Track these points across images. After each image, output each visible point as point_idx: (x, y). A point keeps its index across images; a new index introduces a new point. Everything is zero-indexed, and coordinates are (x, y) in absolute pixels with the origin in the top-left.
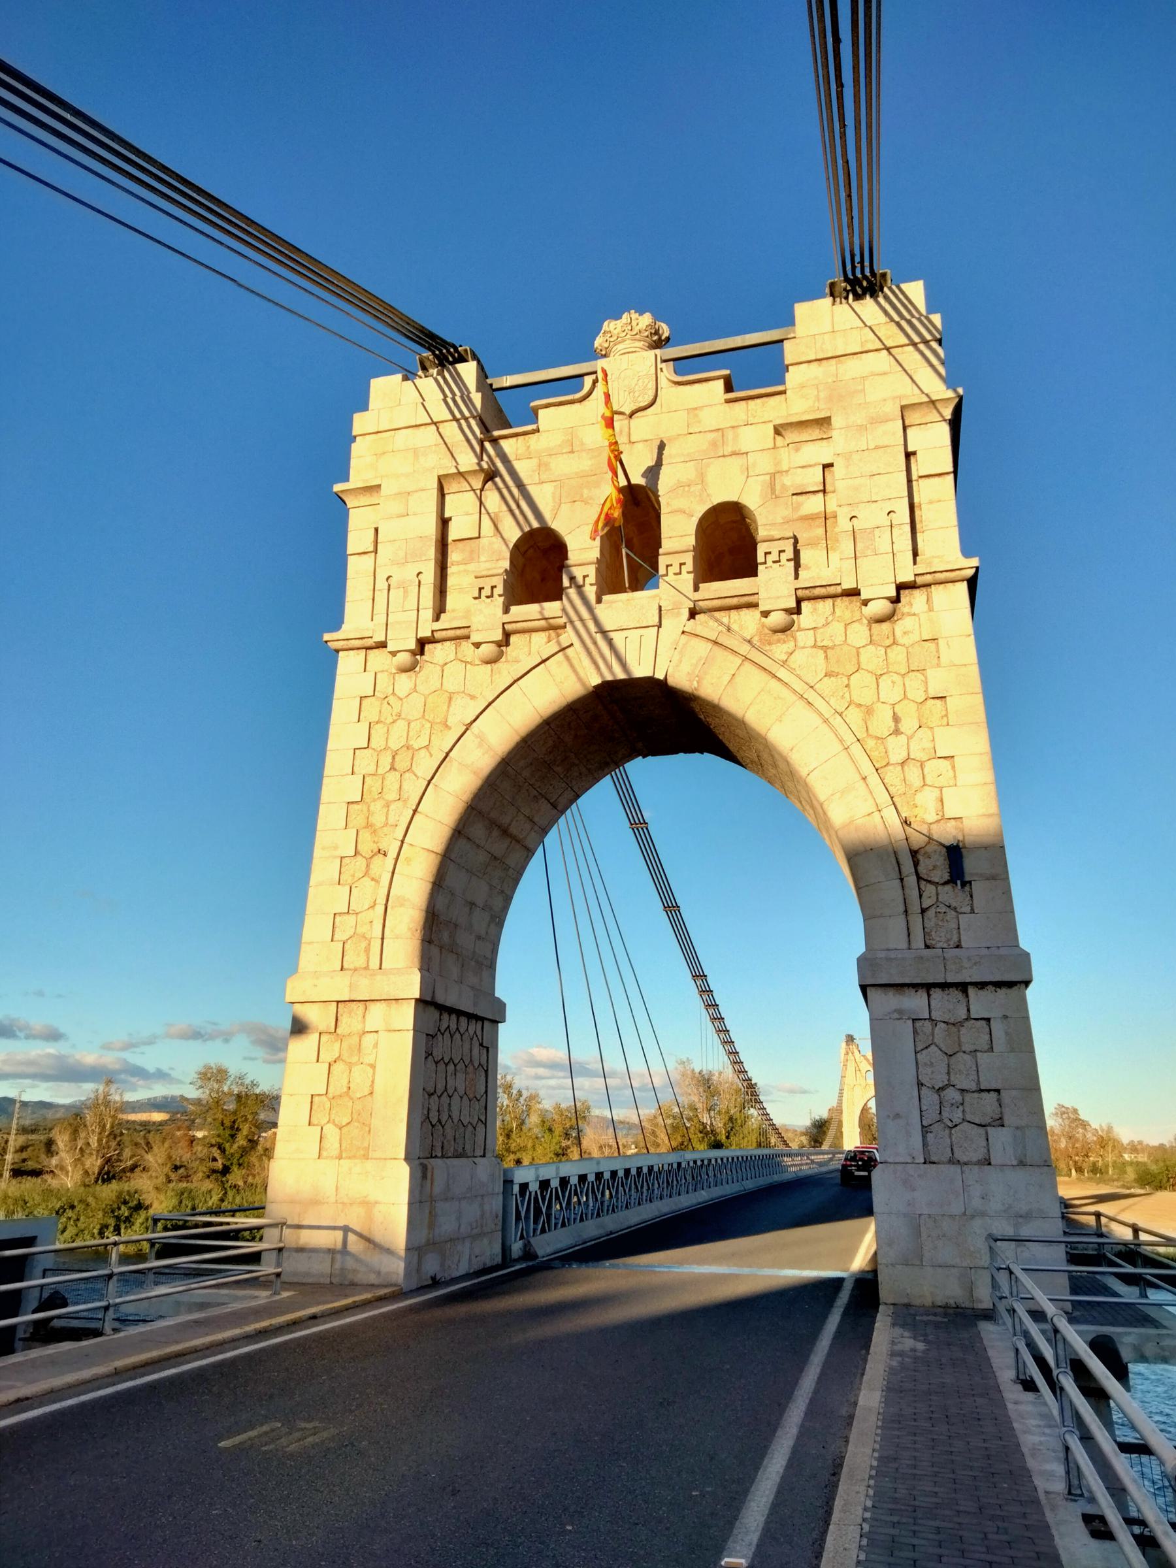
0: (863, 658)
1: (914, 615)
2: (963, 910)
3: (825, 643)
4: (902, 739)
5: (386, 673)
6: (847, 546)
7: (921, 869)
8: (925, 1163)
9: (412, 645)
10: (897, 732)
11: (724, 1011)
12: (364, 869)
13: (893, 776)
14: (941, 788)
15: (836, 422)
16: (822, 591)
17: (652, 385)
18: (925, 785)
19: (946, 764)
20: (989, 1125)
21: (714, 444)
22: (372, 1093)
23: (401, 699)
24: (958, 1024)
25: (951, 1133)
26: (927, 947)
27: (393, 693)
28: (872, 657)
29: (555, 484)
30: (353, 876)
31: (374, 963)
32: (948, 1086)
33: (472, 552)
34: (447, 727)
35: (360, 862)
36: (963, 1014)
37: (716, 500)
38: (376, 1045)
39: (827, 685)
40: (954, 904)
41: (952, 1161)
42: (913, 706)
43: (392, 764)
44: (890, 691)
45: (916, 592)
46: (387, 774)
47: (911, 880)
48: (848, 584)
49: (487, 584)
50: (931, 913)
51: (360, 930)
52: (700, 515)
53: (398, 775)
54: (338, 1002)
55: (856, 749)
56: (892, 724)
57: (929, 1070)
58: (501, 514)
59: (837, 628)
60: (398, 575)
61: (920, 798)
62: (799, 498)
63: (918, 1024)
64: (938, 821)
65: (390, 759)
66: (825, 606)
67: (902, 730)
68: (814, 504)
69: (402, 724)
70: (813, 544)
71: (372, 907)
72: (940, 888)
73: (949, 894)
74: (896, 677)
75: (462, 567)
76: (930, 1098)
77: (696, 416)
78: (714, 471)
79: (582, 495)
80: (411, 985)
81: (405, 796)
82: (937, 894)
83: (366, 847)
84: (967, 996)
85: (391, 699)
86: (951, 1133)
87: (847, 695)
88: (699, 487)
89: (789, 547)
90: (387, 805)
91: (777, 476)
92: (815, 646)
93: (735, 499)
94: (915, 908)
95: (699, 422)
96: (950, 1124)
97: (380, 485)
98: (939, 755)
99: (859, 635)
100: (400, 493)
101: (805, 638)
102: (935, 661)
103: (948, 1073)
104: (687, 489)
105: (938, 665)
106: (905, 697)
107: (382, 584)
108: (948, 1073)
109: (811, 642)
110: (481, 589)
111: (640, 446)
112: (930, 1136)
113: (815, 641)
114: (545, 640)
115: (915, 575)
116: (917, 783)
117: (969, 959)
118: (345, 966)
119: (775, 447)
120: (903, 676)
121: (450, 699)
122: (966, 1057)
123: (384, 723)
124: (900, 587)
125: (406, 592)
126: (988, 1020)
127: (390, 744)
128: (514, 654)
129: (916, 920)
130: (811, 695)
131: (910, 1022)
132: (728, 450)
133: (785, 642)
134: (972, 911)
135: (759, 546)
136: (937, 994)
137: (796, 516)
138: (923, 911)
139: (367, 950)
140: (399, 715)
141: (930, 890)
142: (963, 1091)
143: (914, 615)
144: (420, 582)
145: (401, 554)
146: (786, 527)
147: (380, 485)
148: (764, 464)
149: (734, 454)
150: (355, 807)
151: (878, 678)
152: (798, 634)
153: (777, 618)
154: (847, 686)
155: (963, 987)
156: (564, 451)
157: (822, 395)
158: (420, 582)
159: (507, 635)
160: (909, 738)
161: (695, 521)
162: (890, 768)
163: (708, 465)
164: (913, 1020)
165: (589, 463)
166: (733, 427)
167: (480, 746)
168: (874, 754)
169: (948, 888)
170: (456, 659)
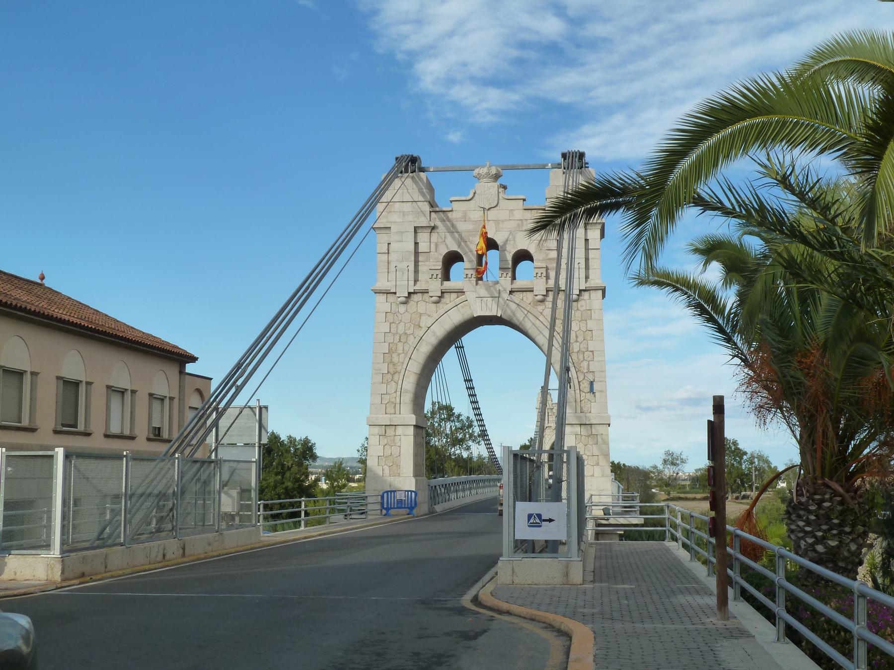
9: (407, 295)
10: (577, 341)
11: (475, 383)
12: (391, 378)
14: (589, 361)
18: (584, 360)
19: (591, 353)
21: (518, 225)
22: (399, 456)
27: (398, 312)
30: (387, 380)
31: (398, 411)
34: (420, 327)
35: (389, 376)
38: (400, 440)
42: (582, 333)
43: (400, 339)
45: (586, 292)
50: (583, 402)
54: (385, 425)
56: (575, 338)
58: (438, 243)
60: (399, 265)
63: (577, 436)
64: (587, 372)
67: (578, 340)
73: (589, 396)
74: (577, 322)
75: (423, 263)
77: (512, 213)
81: (405, 352)
83: (391, 371)
89: (544, 271)
90: (399, 355)
95: (513, 215)
97: (390, 227)
100: (399, 232)
105: (591, 319)
106: (580, 329)
107: (392, 268)
111: (491, 222)
114: (456, 296)
116: (582, 359)
118: (387, 413)
120: (580, 321)
121: (420, 316)
125: (403, 273)
127: (398, 332)
128: (444, 300)
134: (595, 402)
139: (395, 407)
140: (401, 320)
142: (588, 456)
150: (386, 355)
152: (546, 303)
153: (540, 297)
159: (442, 293)
162: (574, 353)
163: (517, 233)
165: (472, 226)
167: (434, 335)
169: (589, 394)
170: (422, 300)
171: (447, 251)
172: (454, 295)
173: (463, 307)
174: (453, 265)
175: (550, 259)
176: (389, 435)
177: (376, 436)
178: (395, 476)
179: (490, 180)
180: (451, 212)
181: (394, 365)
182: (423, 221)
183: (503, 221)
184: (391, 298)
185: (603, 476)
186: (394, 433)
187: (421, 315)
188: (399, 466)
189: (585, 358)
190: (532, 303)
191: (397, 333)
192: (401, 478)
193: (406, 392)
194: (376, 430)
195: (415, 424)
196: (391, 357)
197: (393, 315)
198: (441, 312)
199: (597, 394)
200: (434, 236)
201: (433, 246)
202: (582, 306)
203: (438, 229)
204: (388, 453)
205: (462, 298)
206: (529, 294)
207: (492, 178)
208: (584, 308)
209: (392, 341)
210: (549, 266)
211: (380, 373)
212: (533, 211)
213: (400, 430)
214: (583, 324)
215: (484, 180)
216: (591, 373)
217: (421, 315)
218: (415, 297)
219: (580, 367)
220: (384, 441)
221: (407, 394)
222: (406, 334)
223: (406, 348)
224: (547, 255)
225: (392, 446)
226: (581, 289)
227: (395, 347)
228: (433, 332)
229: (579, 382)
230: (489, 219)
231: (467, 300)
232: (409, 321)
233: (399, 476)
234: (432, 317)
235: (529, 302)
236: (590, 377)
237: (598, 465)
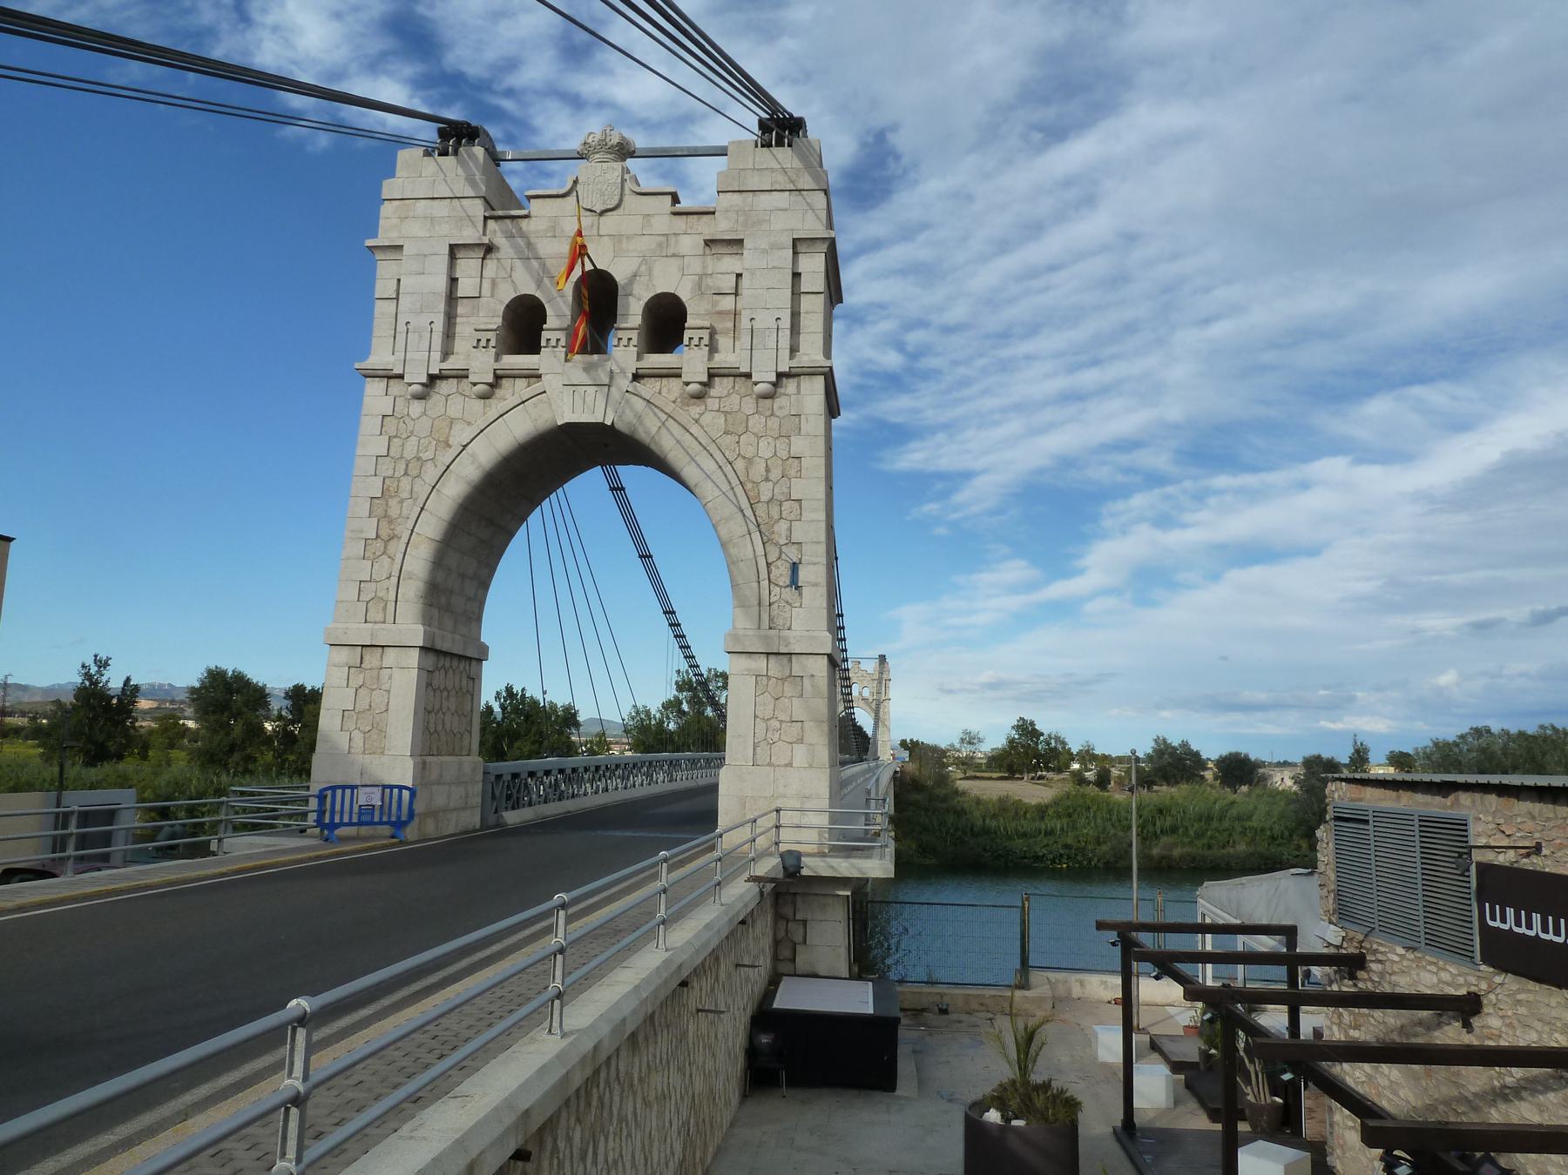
0: (751, 423)
1: (788, 395)
2: (795, 605)
3: (726, 409)
6: (745, 340)
9: (424, 380)
10: (767, 479)
11: (690, 640)
12: (382, 549)
14: (791, 521)
16: (727, 371)
17: (618, 192)
19: (796, 505)
20: (794, 743)
21: (660, 245)
22: (387, 710)
25: (771, 748)
27: (408, 415)
28: (756, 423)
30: (374, 553)
31: (390, 618)
32: (773, 718)
34: (449, 446)
35: (379, 544)
38: (390, 678)
40: (790, 601)
41: (770, 764)
44: (765, 450)
45: (791, 380)
49: (484, 336)
50: (775, 606)
51: (380, 594)
52: (646, 300)
53: (410, 478)
54: (363, 646)
56: (764, 473)
57: (762, 708)
59: (735, 398)
61: (776, 528)
62: (718, 297)
66: (728, 382)
67: (771, 478)
68: (727, 303)
69: (413, 439)
70: (726, 333)
71: (389, 578)
72: (783, 589)
73: (789, 594)
74: (770, 440)
75: (465, 319)
76: (761, 726)
77: (649, 220)
78: (659, 266)
80: (415, 633)
81: (415, 496)
82: (781, 594)
83: (384, 533)
85: (407, 420)
86: (771, 748)
87: (737, 449)
88: (647, 277)
89: (705, 334)
90: (402, 502)
91: (704, 277)
95: (651, 226)
97: (402, 246)
98: (792, 498)
99: (749, 405)
101: (712, 403)
102: (797, 431)
103: (774, 710)
105: (799, 434)
107: (401, 327)
108: (774, 710)
110: (479, 340)
111: (606, 238)
114: (526, 384)
115: (790, 368)
116: (776, 517)
117: (794, 637)
118: (368, 620)
119: (704, 255)
120: (775, 439)
121: (451, 423)
122: (786, 700)
123: (400, 438)
124: (780, 375)
125: (420, 336)
127: (405, 455)
130: (712, 448)
132: (670, 252)
133: (698, 406)
135: (686, 331)
136: (772, 659)
139: (385, 609)
140: (412, 432)
141: (776, 590)
142: (781, 722)
143: (788, 395)
144: (432, 329)
145: (418, 305)
146: (707, 317)
147: (402, 246)
148: (695, 266)
149: (674, 255)
152: (710, 400)
153: (694, 388)
157: (741, 219)
158: (432, 329)
160: (775, 484)
162: (760, 504)
166: (674, 234)
168: (751, 494)
169: (788, 589)
170: (458, 392)
171: (514, 295)
172: (521, 383)
175: (720, 313)
176: (369, 667)
178: (374, 753)
179: (609, 156)
180: (527, 220)
182: (470, 235)
183: (629, 238)
185: (811, 766)
186: (378, 663)
187: (452, 421)
188: (383, 733)
190: (679, 400)
191: (402, 458)
193: (410, 578)
194: (343, 655)
195: (421, 645)
196: (387, 504)
197: (397, 421)
199: (805, 590)
200: (491, 264)
201: (486, 285)
202: (780, 408)
203: (498, 252)
204: (363, 704)
205: (537, 387)
206: (674, 384)
207: (611, 153)
208: (786, 412)
209: (390, 473)
210: (718, 326)
212: (690, 217)
213: (391, 656)
214: (781, 445)
215: (597, 156)
216: (796, 546)
217: (452, 421)
218: (444, 387)
219: (773, 532)
220: (357, 679)
221: (411, 581)
222: (419, 459)
224: (714, 304)
225: (373, 690)
226: (779, 370)
227: (395, 485)
229: (768, 564)
230: (601, 233)
231: (545, 392)
232: (428, 434)
233: (382, 753)
236: (792, 554)
237: (802, 743)
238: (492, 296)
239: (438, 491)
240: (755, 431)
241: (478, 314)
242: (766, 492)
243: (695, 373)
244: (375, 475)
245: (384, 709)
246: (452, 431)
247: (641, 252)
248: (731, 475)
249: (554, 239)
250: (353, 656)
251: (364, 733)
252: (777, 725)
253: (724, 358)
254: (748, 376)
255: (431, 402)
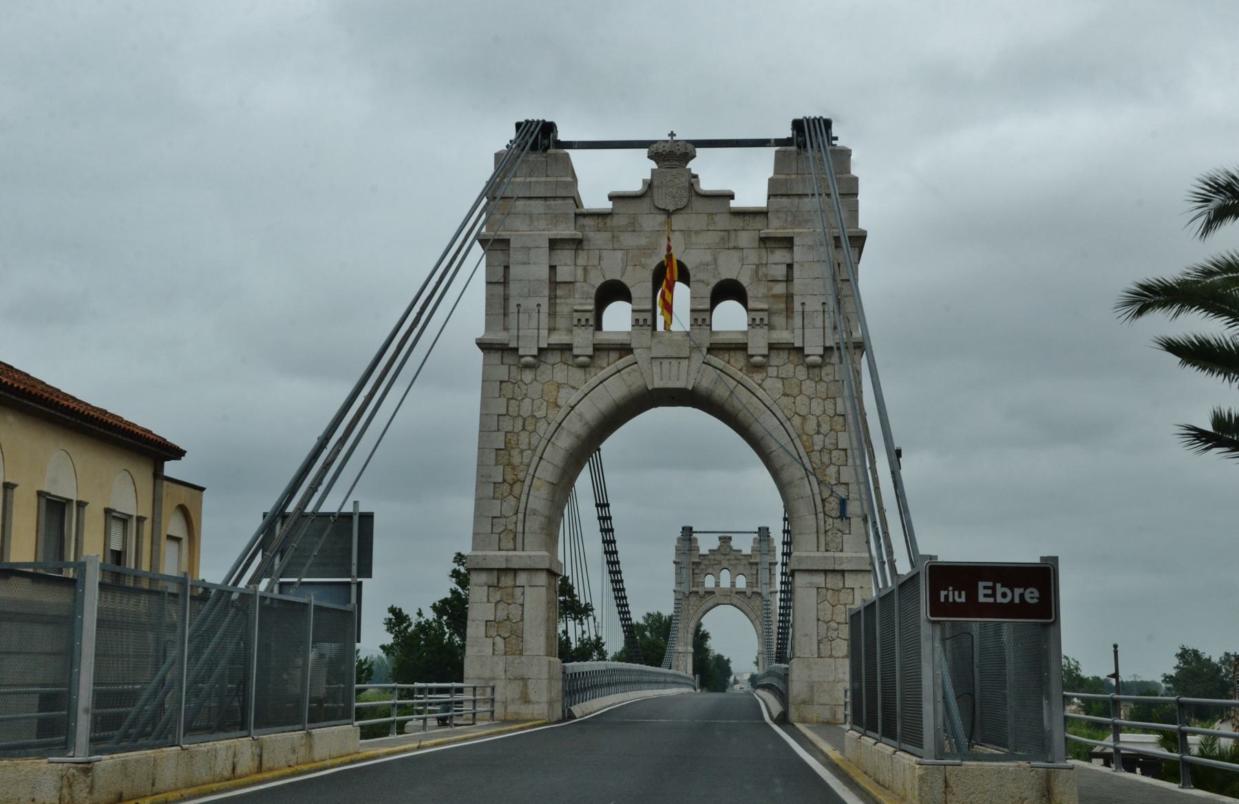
0: (804, 387)
3: (783, 376)
4: (821, 437)
5: (515, 367)
7: (826, 509)
8: (818, 657)
9: (535, 352)
10: (818, 433)
12: (509, 490)
13: (816, 457)
14: (839, 466)
15: (797, 241)
16: (784, 346)
19: (842, 453)
21: (722, 239)
22: (522, 620)
23: (526, 384)
24: (839, 591)
26: (827, 551)
28: (808, 387)
29: (623, 251)
30: (502, 494)
32: (832, 621)
33: (570, 291)
35: (506, 487)
36: (841, 586)
37: (723, 278)
38: (523, 594)
39: (785, 400)
40: (841, 529)
41: (831, 656)
42: (828, 418)
43: (524, 426)
44: (817, 408)
46: (521, 433)
47: (821, 516)
48: (798, 344)
50: (829, 533)
52: (713, 285)
53: (528, 433)
55: (797, 442)
56: (816, 428)
58: (588, 267)
62: (773, 284)
63: (820, 590)
64: (836, 484)
65: (521, 423)
66: (784, 355)
69: (527, 401)
70: (777, 312)
71: (516, 513)
72: (835, 520)
73: (838, 523)
74: (820, 401)
75: (563, 301)
76: (823, 626)
77: (713, 219)
78: (723, 257)
79: (641, 262)
82: (833, 523)
83: (509, 478)
84: (844, 577)
90: (522, 452)
91: (760, 266)
92: (777, 377)
93: (735, 278)
94: (822, 530)
95: (714, 223)
96: (831, 639)
98: (839, 447)
99: (802, 373)
100: (523, 248)
101: (772, 371)
103: (832, 615)
104: (706, 267)
109: (775, 374)
111: (677, 234)
112: (821, 645)
113: (778, 374)
117: (846, 558)
118: (501, 548)
120: (824, 400)
121: (558, 388)
123: (517, 400)
125: (530, 316)
126: (853, 589)
128: (598, 362)
129: (822, 537)
131: (815, 589)
132: (731, 245)
134: (850, 534)
136: (830, 576)
137: (769, 295)
138: (826, 532)
139: (514, 539)
140: (526, 395)
141: (830, 521)
142: (838, 623)
144: (539, 311)
145: (526, 290)
146: (764, 300)
149: (735, 248)
150: (502, 452)
151: (811, 399)
154: (794, 403)
155: (843, 572)
156: (629, 230)
157: (789, 219)
158: (539, 311)
161: (710, 288)
162: (814, 453)
164: (818, 588)
166: (735, 230)
167: (580, 420)
169: (839, 520)
170: (562, 361)
172: (614, 355)
173: (629, 374)
174: (612, 302)
175: (774, 296)
176: (505, 585)
177: (483, 588)
178: (514, 654)
181: (514, 468)
183: (697, 232)
184: (509, 359)
186: (512, 583)
187: (559, 386)
188: (520, 637)
189: (834, 460)
190: (744, 369)
192: (523, 658)
193: (534, 514)
196: (510, 455)
197: (511, 386)
198: (593, 381)
199: (853, 520)
201: (580, 272)
202: (827, 375)
204: (501, 615)
205: (628, 359)
209: (510, 429)
211: (490, 482)
213: (522, 579)
217: (559, 386)
219: (825, 475)
221: (535, 517)
222: (534, 416)
223: (534, 441)
224: (770, 289)
225: (508, 604)
227: (515, 439)
228: (579, 415)
229: (823, 501)
232: (540, 396)
233: (521, 654)
234: (578, 389)
235: (740, 368)
236: (841, 491)
238: (585, 281)
239: (553, 443)
240: (808, 393)
241: (574, 295)
242: (818, 441)
243: (759, 347)
244: (498, 430)
245: (519, 619)
246: (559, 394)
247: (708, 244)
248: (791, 430)
249: (634, 233)
250: (493, 579)
251: (505, 639)
252: (835, 625)
253: (782, 336)
254: (801, 349)
255: (539, 372)
